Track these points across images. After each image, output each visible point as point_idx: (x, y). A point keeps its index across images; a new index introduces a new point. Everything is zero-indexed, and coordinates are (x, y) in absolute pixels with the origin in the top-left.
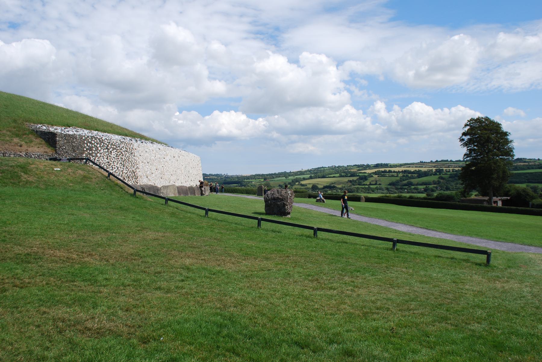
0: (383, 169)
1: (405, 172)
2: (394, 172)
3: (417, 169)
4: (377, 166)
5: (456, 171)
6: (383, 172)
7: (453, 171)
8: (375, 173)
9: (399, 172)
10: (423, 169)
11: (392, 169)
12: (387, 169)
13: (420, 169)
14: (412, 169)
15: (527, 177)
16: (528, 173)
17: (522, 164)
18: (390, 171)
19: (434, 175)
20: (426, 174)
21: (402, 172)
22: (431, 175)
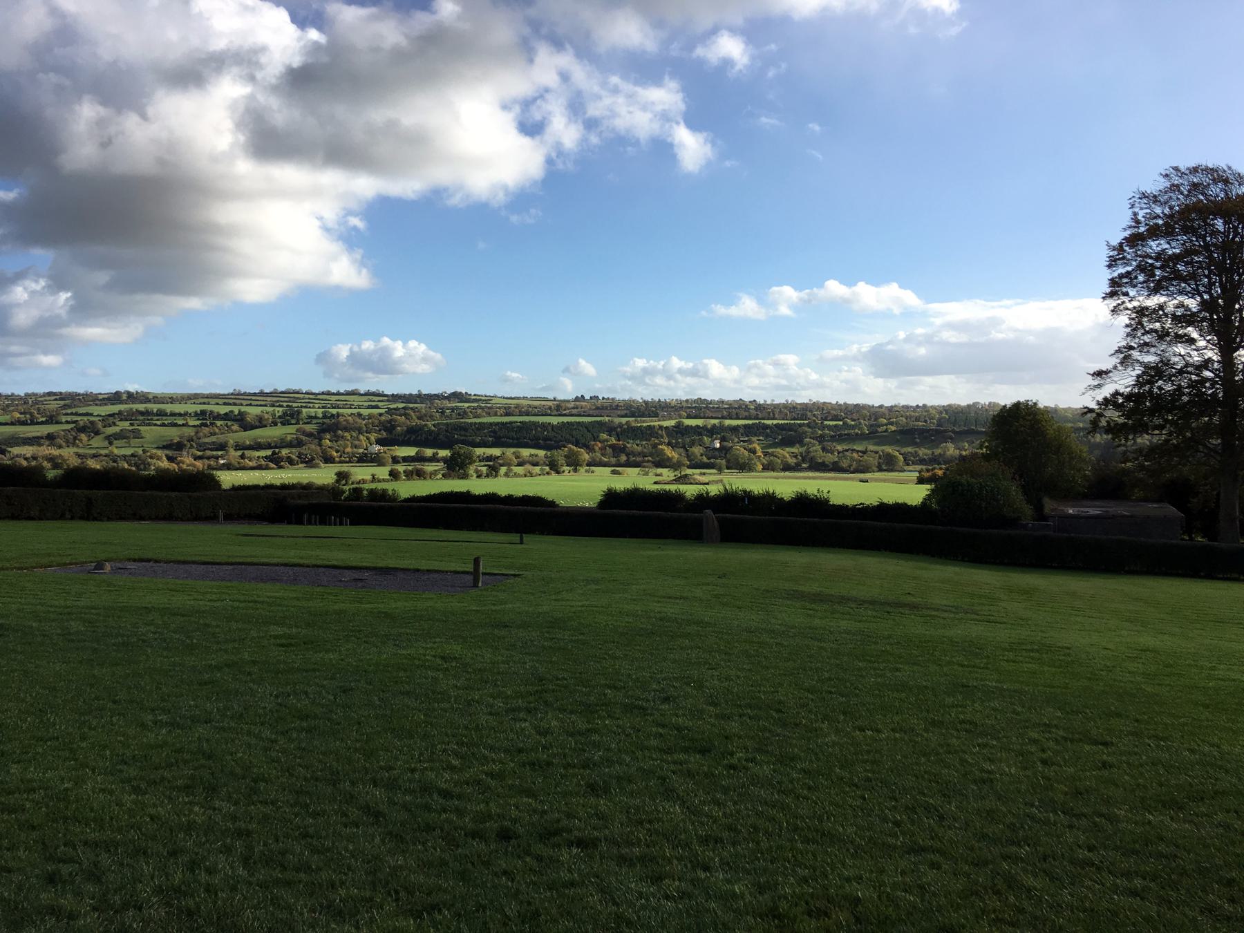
0: (141, 407)
1: (203, 412)
2: (173, 414)
3: (236, 410)
4: (116, 397)
5: (333, 416)
6: (142, 413)
7: (325, 416)
8: (120, 415)
9: (186, 414)
10: (254, 411)
11: (169, 408)
12: (155, 407)
13: (243, 409)
14: (223, 410)
15: (495, 432)
16: (497, 424)
17: (466, 405)
18: (161, 413)
19: (283, 424)
20: (260, 423)
21: (196, 414)
22: (275, 424)
